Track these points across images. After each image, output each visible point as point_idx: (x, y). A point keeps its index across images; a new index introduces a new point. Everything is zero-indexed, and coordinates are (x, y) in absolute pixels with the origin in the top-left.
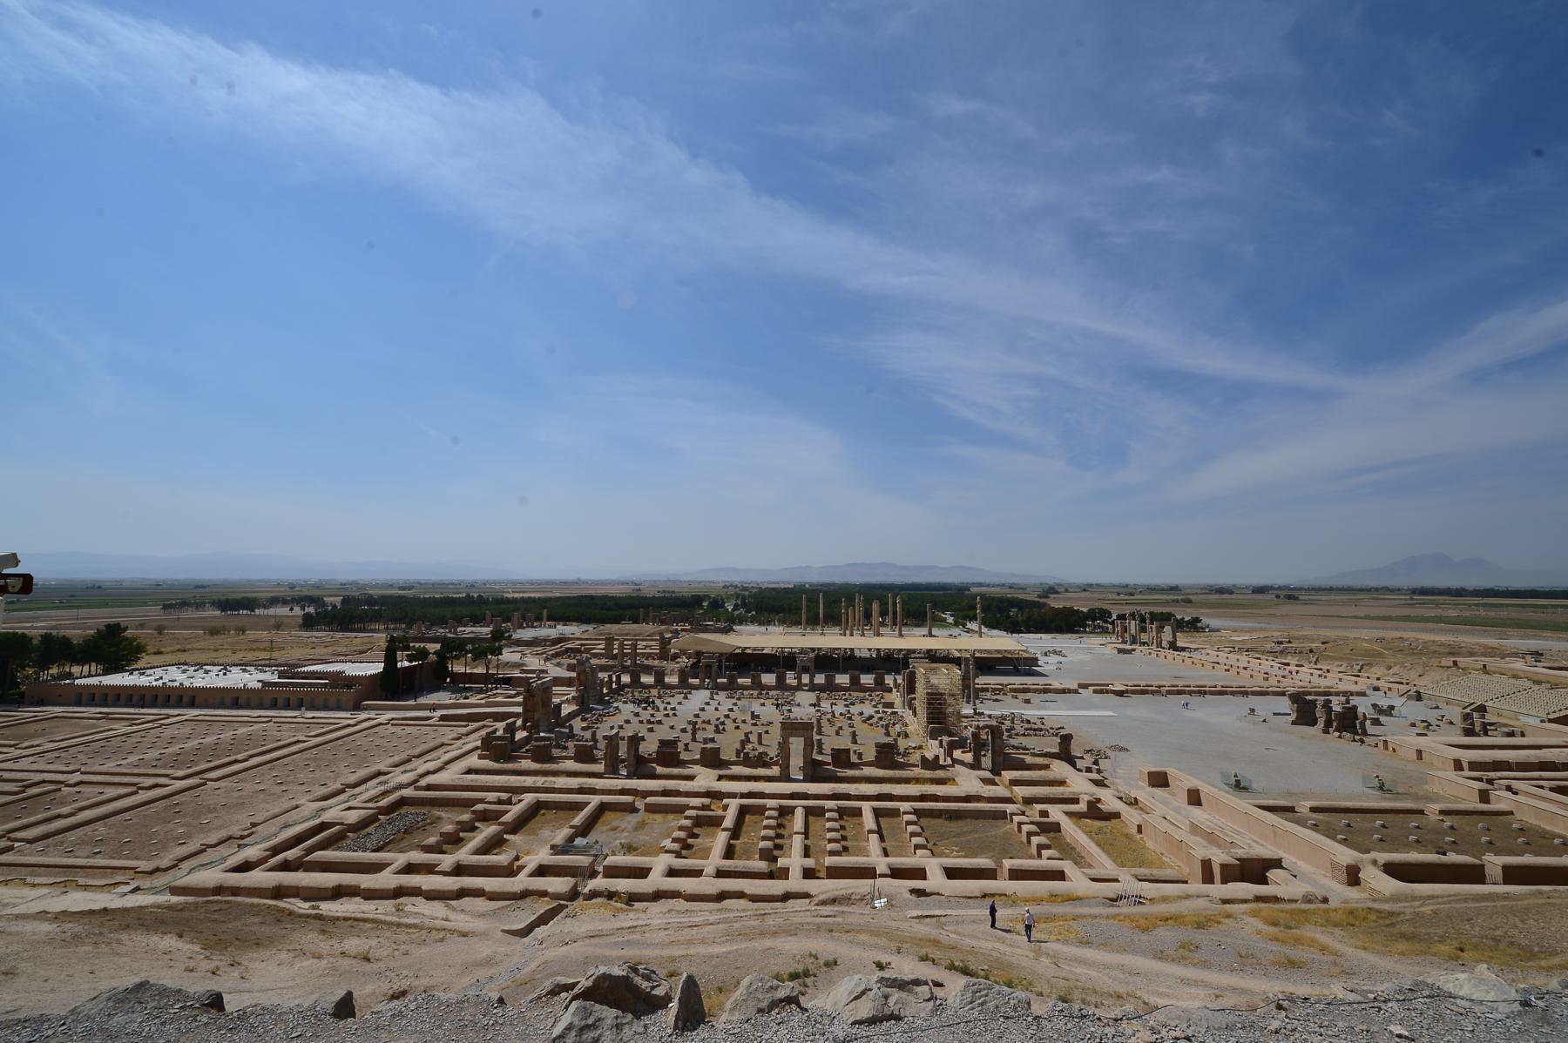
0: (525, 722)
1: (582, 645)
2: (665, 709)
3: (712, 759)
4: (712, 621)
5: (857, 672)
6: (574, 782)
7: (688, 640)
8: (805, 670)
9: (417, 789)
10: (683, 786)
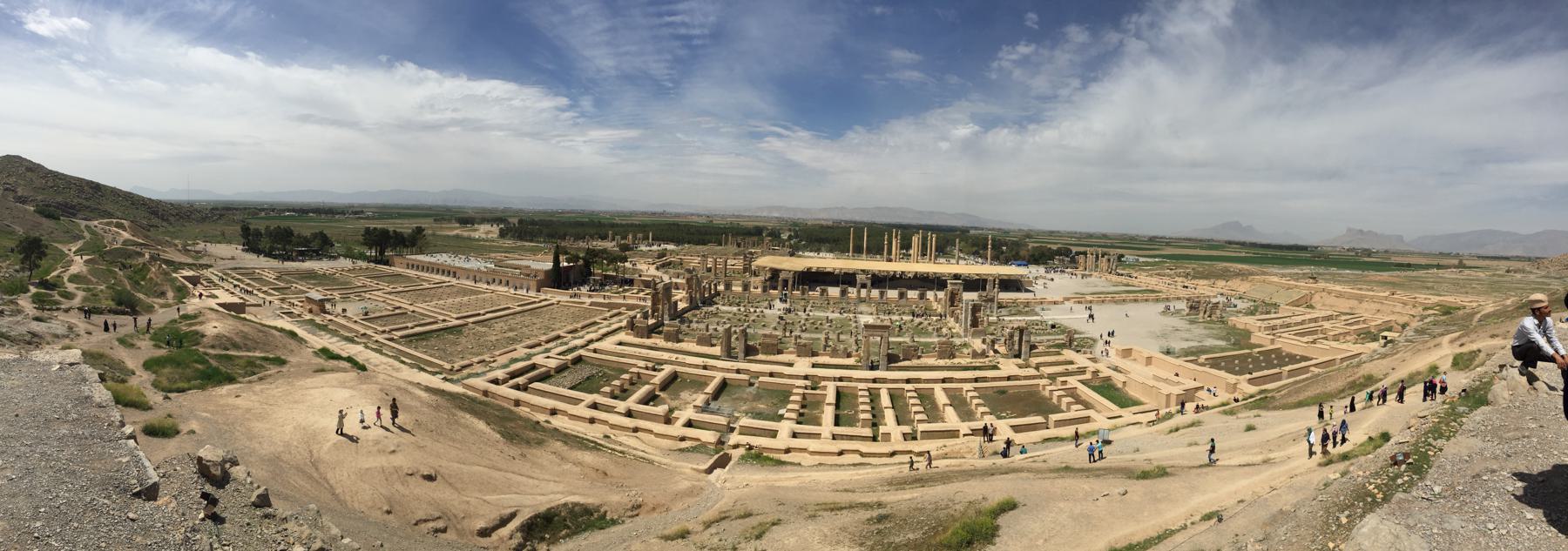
0: (653, 312)
2: (755, 312)
3: (807, 351)
5: (904, 290)
6: (699, 361)
7: (766, 261)
8: (864, 286)
9: (589, 350)
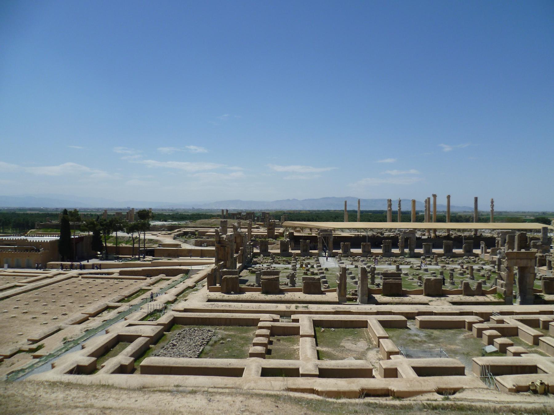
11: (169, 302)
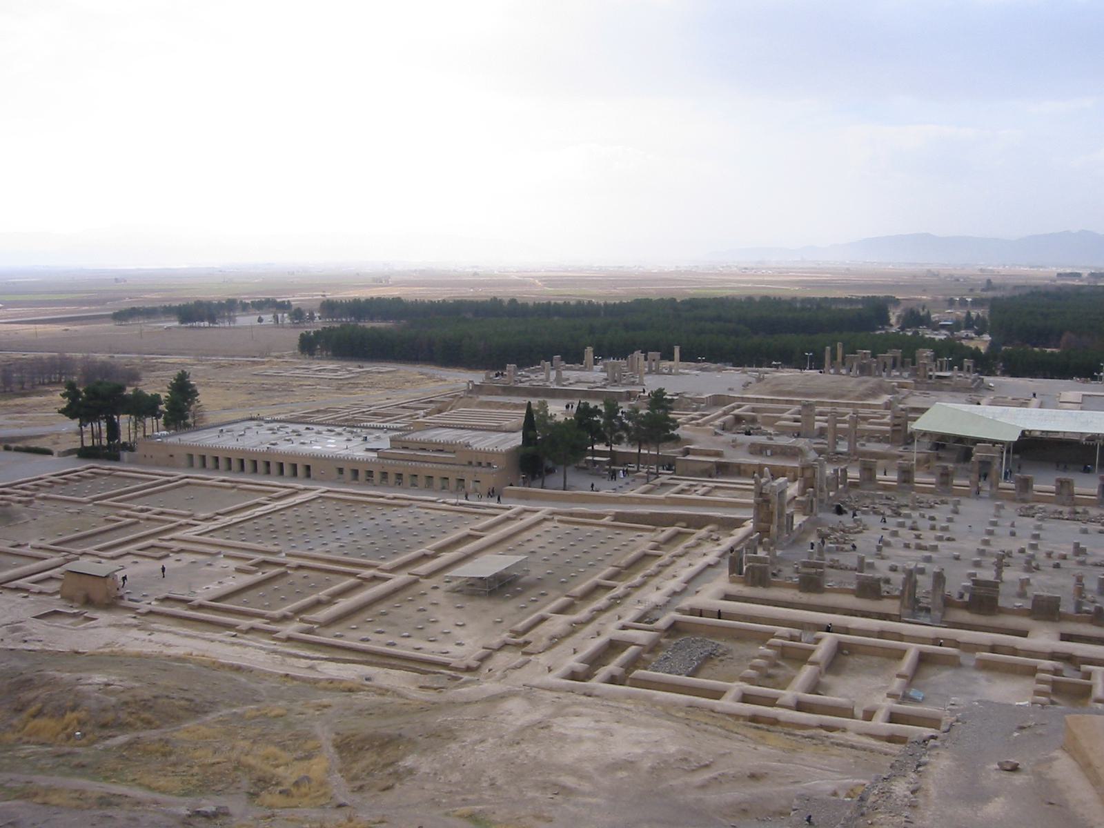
1: (753, 410)
4: (951, 369)
10: (1019, 642)
11: (674, 594)
